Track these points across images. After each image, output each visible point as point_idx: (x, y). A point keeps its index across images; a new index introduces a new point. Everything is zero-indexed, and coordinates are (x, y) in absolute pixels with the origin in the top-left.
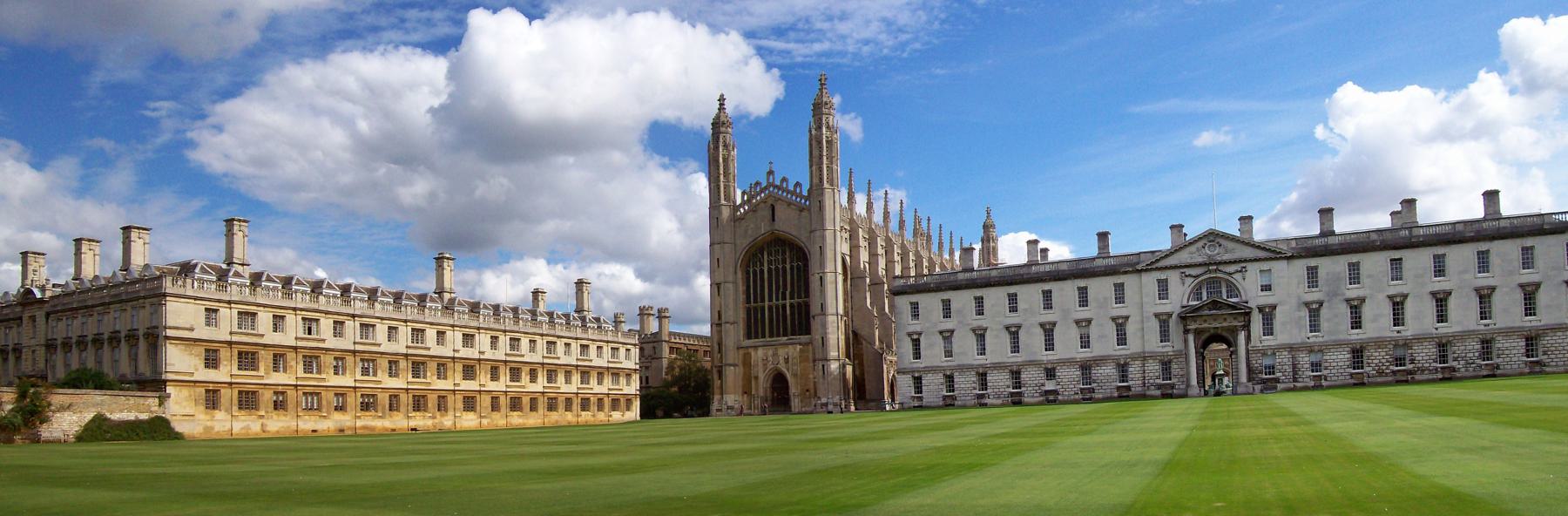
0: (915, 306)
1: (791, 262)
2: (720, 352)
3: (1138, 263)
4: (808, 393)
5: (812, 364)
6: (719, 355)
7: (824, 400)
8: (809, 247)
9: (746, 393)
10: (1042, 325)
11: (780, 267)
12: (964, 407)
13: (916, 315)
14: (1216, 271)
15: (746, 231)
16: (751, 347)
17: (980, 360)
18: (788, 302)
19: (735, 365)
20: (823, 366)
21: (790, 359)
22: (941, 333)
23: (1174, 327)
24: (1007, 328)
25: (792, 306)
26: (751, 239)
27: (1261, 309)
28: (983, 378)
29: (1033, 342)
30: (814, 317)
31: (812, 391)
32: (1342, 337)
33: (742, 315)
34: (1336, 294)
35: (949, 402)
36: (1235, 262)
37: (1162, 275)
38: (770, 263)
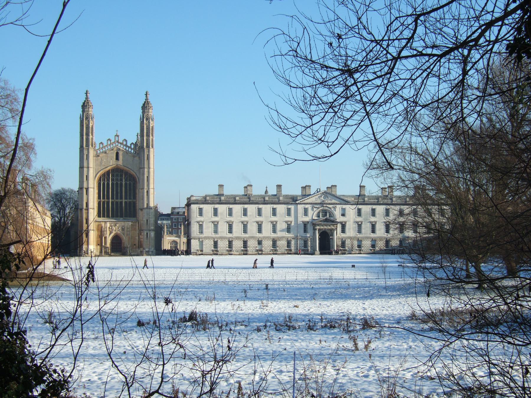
0: (201, 210)
1: (126, 180)
2: (86, 223)
3: (297, 200)
4: (135, 246)
5: (138, 232)
6: (86, 225)
7: (147, 250)
8: (138, 175)
9: (99, 245)
10: (257, 222)
11: (119, 182)
12: (222, 255)
13: (201, 214)
14: (326, 206)
15: (101, 163)
16: (102, 222)
17: (230, 235)
18: (124, 201)
19: (93, 230)
20: (147, 233)
21: (126, 229)
22: (213, 222)
23: (310, 228)
24: (242, 222)
25: (126, 203)
26: (105, 167)
27: (341, 223)
28: (230, 243)
29: (253, 228)
30: (142, 210)
31: (137, 245)
32: (368, 235)
33: (96, 205)
34: (367, 220)
35: (215, 252)
36: (333, 204)
37: (307, 206)
38: (112, 180)
